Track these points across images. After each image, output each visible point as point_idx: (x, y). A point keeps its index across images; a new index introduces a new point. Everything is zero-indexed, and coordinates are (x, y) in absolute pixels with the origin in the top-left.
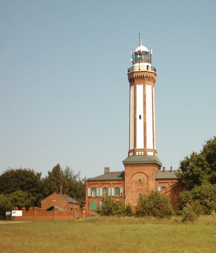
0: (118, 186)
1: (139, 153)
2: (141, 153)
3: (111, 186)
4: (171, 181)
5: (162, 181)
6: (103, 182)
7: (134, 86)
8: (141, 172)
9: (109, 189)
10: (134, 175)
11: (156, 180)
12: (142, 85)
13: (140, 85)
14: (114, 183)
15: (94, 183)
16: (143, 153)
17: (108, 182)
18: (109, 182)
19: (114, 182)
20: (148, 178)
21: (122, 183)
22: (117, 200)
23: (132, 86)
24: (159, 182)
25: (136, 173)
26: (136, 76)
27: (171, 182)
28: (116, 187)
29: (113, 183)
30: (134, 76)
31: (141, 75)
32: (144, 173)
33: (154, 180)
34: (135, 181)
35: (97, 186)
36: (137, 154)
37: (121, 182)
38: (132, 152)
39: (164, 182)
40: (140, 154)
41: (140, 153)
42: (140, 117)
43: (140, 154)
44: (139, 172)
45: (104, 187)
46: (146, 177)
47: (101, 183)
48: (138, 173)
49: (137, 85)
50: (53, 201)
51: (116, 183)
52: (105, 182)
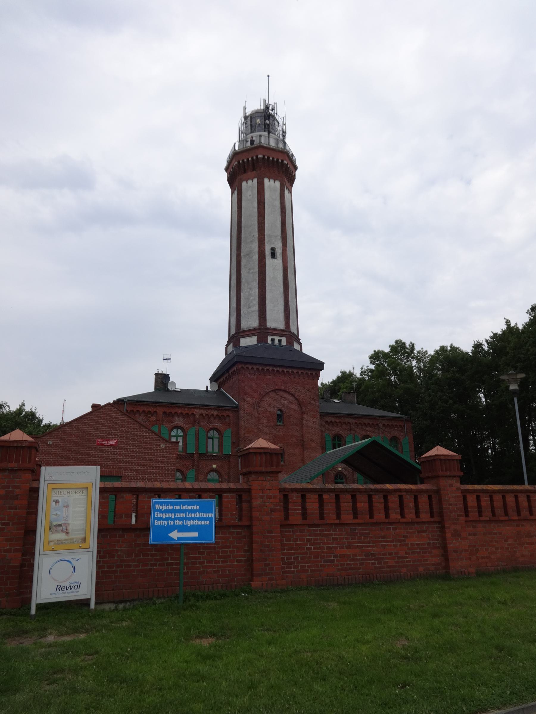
0: (218, 425)
1: (273, 340)
2: (280, 341)
3: (197, 423)
4: (356, 421)
5: (334, 420)
6: (173, 411)
7: (255, 181)
8: (283, 388)
9: (192, 432)
10: (264, 397)
11: (320, 416)
12: (278, 183)
13: (272, 181)
14: (207, 415)
15: (141, 409)
16: (284, 340)
17: (187, 410)
18: (190, 411)
19: (205, 412)
20: (301, 407)
21: (228, 416)
22: (214, 466)
23: (250, 182)
24: (327, 422)
25: (270, 390)
26: (264, 156)
27: (356, 423)
28: (211, 426)
29: (202, 415)
30: (260, 156)
31: (278, 160)
32: (293, 391)
33: (319, 414)
34: (268, 413)
35: (153, 419)
36: (270, 342)
37: (226, 413)
38: (253, 335)
39: (340, 422)
40: (277, 342)
41: (277, 339)
42: (273, 255)
43: (277, 342)
44: (277, 388)
45: (172, 425)
46: (295, 406)
47: (165, 413)
48: (275, 390)
49: (266, 180)
50: (100, 442)
51: (212, 415)
52: (179, 411)
